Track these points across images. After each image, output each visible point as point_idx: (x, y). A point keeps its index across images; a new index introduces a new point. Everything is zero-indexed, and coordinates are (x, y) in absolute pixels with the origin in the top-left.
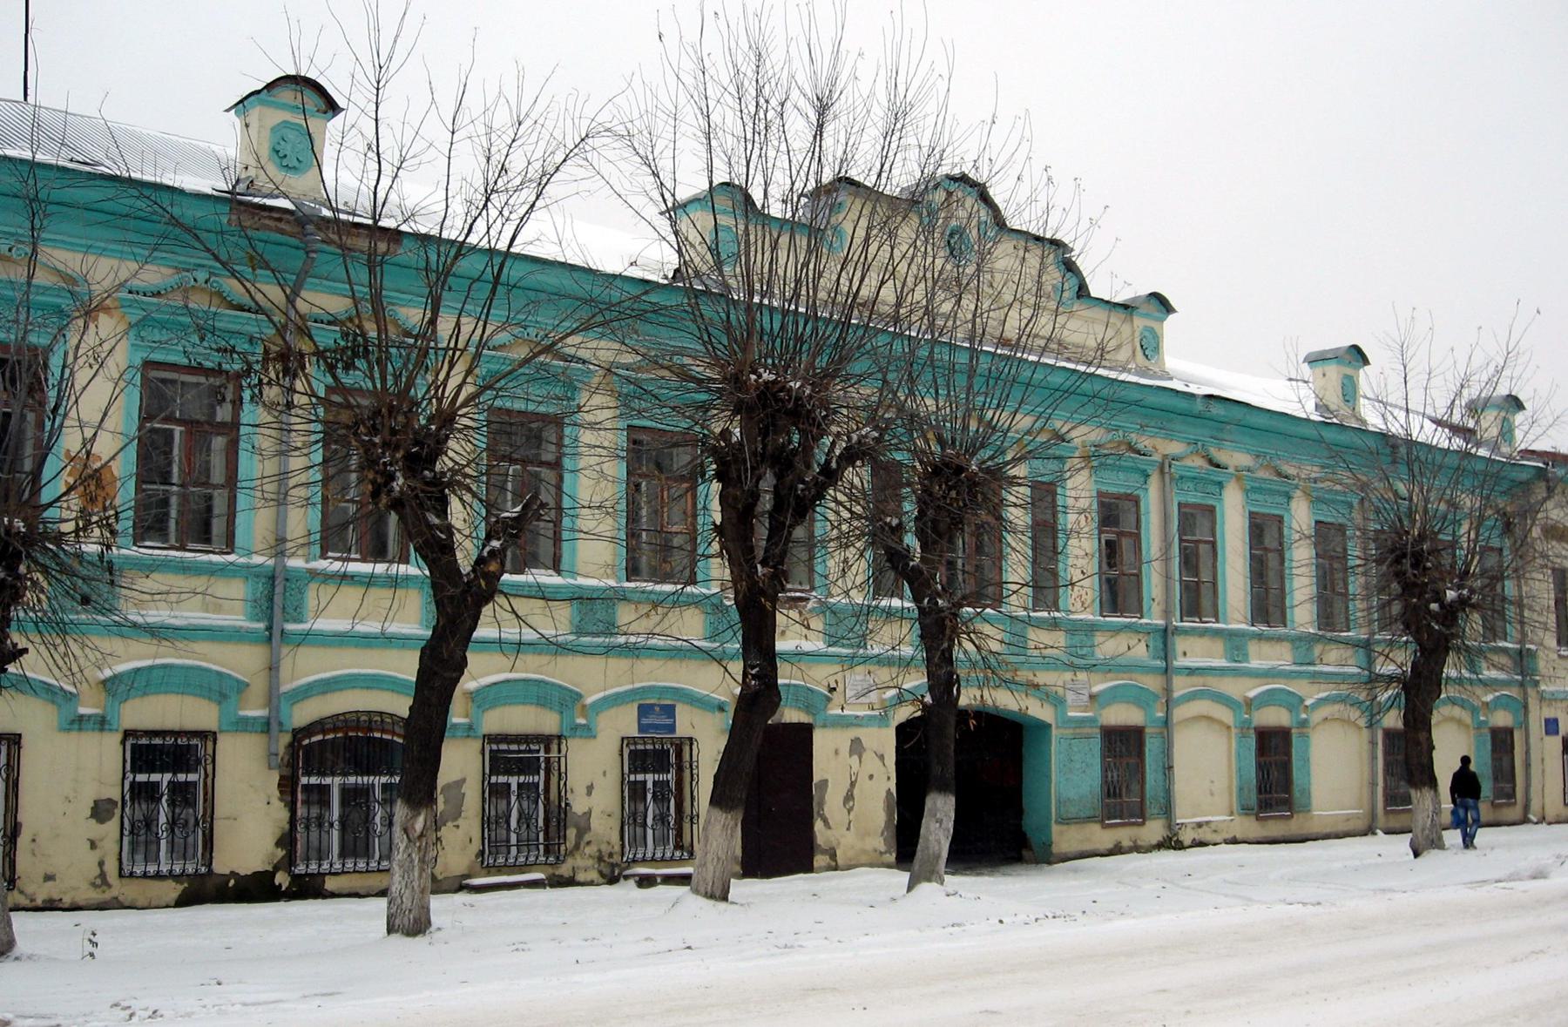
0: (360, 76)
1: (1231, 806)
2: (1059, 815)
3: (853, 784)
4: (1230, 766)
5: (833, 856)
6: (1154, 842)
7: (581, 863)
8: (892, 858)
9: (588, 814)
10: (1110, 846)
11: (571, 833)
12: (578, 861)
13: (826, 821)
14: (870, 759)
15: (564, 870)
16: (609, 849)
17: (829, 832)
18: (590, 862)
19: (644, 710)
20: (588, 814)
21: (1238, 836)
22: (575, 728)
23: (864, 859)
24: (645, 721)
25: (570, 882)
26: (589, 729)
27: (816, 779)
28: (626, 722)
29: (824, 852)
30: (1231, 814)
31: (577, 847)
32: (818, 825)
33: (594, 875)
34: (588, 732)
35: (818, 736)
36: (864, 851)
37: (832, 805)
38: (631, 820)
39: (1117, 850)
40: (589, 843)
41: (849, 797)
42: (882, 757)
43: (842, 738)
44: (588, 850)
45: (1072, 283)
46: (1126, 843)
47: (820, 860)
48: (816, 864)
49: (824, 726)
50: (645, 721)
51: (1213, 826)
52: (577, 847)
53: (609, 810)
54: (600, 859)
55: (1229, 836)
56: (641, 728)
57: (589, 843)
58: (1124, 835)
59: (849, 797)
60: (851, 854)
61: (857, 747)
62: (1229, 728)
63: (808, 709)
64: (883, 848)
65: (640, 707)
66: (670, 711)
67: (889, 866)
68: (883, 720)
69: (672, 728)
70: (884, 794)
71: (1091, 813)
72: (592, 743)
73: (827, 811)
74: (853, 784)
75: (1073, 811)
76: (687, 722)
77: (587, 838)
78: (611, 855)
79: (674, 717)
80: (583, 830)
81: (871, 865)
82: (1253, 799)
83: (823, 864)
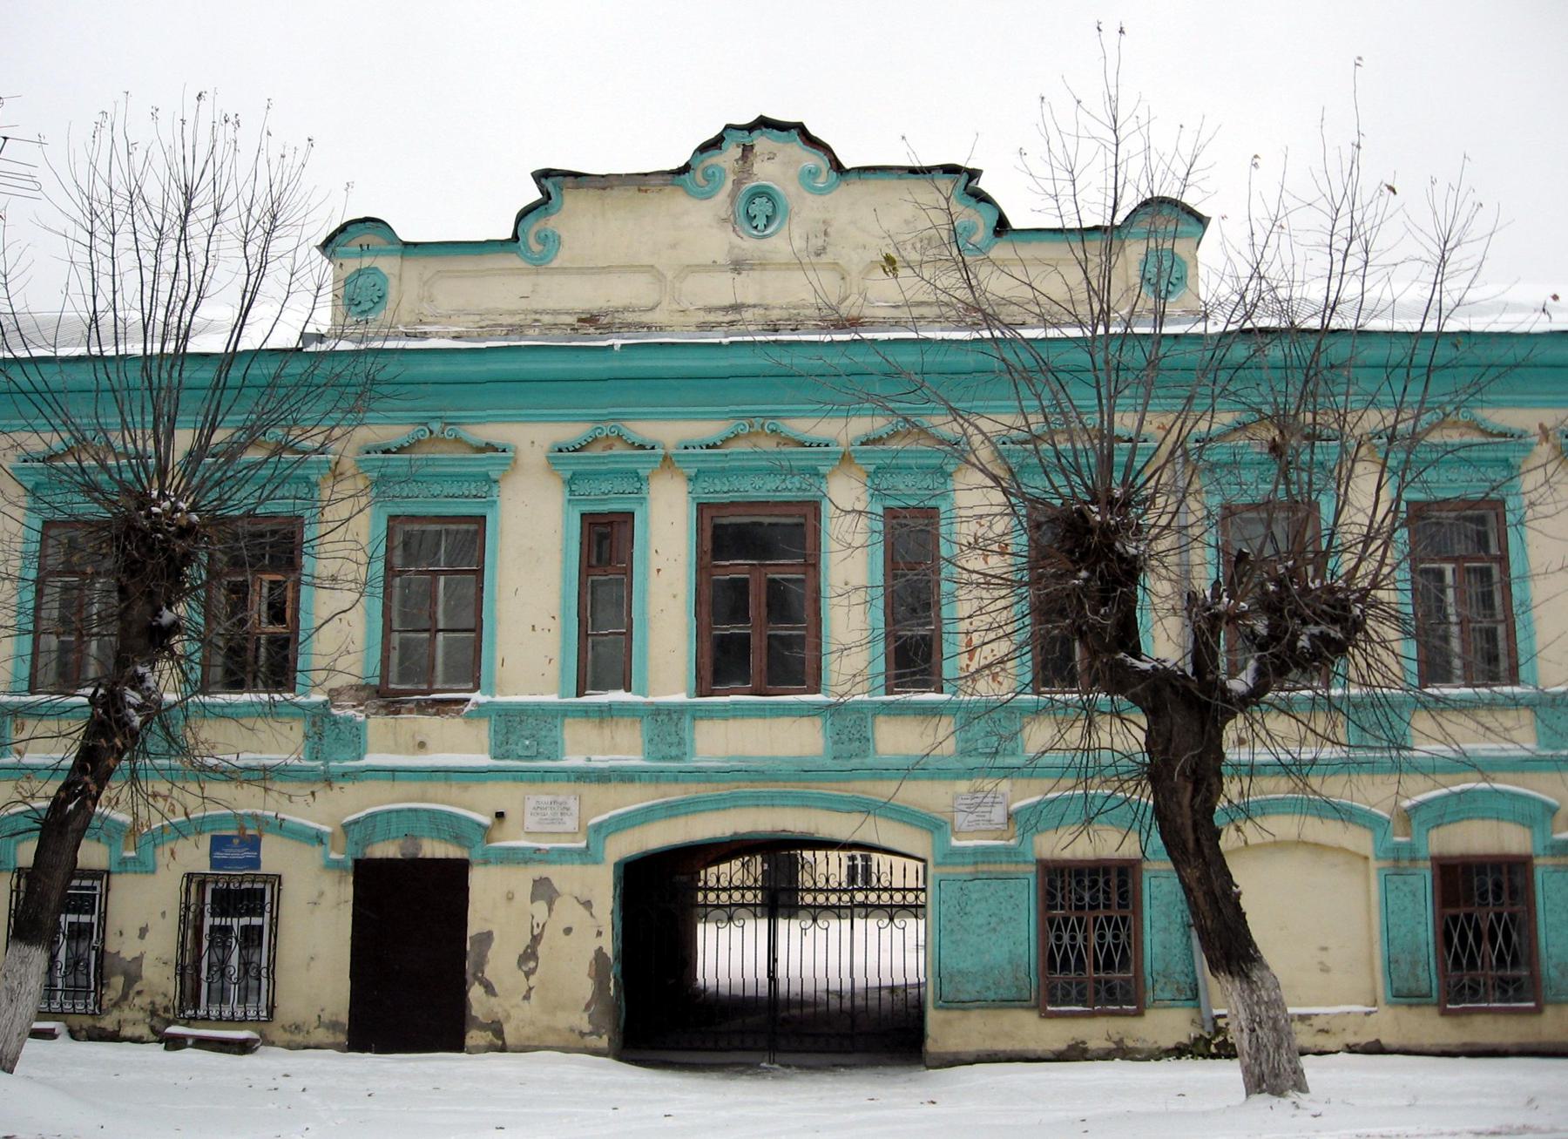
0: (74, 287)
1: (1374, 990)
2: (940, 996)
3: (536, 939)
4: (1370, 927)
5: (498, 1031)
6: (1169, 1043)
7: (132, 1017)
8: (603, 1042)
9: (138, 960)
10: (1061, 1046)
11: (118, 982)
12: (127, 1013)
13: (489, 988)
14: (567, 911)
15: (108, 1023)
16: (165, 1002)
17: (493, 999)
18: (141, 1015)
19: (218, 843)
20: (138, 960)
21: (1386, 1040)
22: (124, 862)
23: (551, 1039)
24: (218, 855)
25: (114, 1037)
26: (143, 864)
27: (473, 929)
28: (196, 856)
29: (483, 1027)
30: (1375, 1004)
31: (125, 996)
32: (475, 993)
33: (143, 1030)
34: (144, 867)
35: (478, 880)
36: (552, 1029)
37: (500, 963)
38: (187, 971)
39: (1076, 1053)
40: (139, 993)
41: (529, 955)
42: (587, 905)
43: (522, 879)
44: (137, 1001)
45: (982, 221)
46: (1093, 1044)
47: (474, 1037)
48: (469, 1042)
49: (486, 862)
50: (218, 855)
51: (1318, 1023)
52: (125, 996)
53: (165, 958)
54: (153, 1013)
55: (1363, 1039)
56: (215, 863)
57: (139, 993)
58: (1095, 1031)
59: (529, 955)
60: (528, 1031)
61: (544, 890)
62: (1366, 858)
63: (458, 839)
64: (587, 1028)
65: (214, 839)
66: (254, 843)
67: (596, 1052)
68: (586, 856)
69: (256, 863)
70: (592, 955)
71: (1013, 993)
72: (150, 879)
73: (489, 973)
74: (536, 939)
75: (970, 990)
76: (274, 856)
77: (138, 987)
78: (166, 1009)
79: (258, 850)
80: (132, 976)
81: (565, 1050)
82: (1428, 977)
83: (483, 1043)
